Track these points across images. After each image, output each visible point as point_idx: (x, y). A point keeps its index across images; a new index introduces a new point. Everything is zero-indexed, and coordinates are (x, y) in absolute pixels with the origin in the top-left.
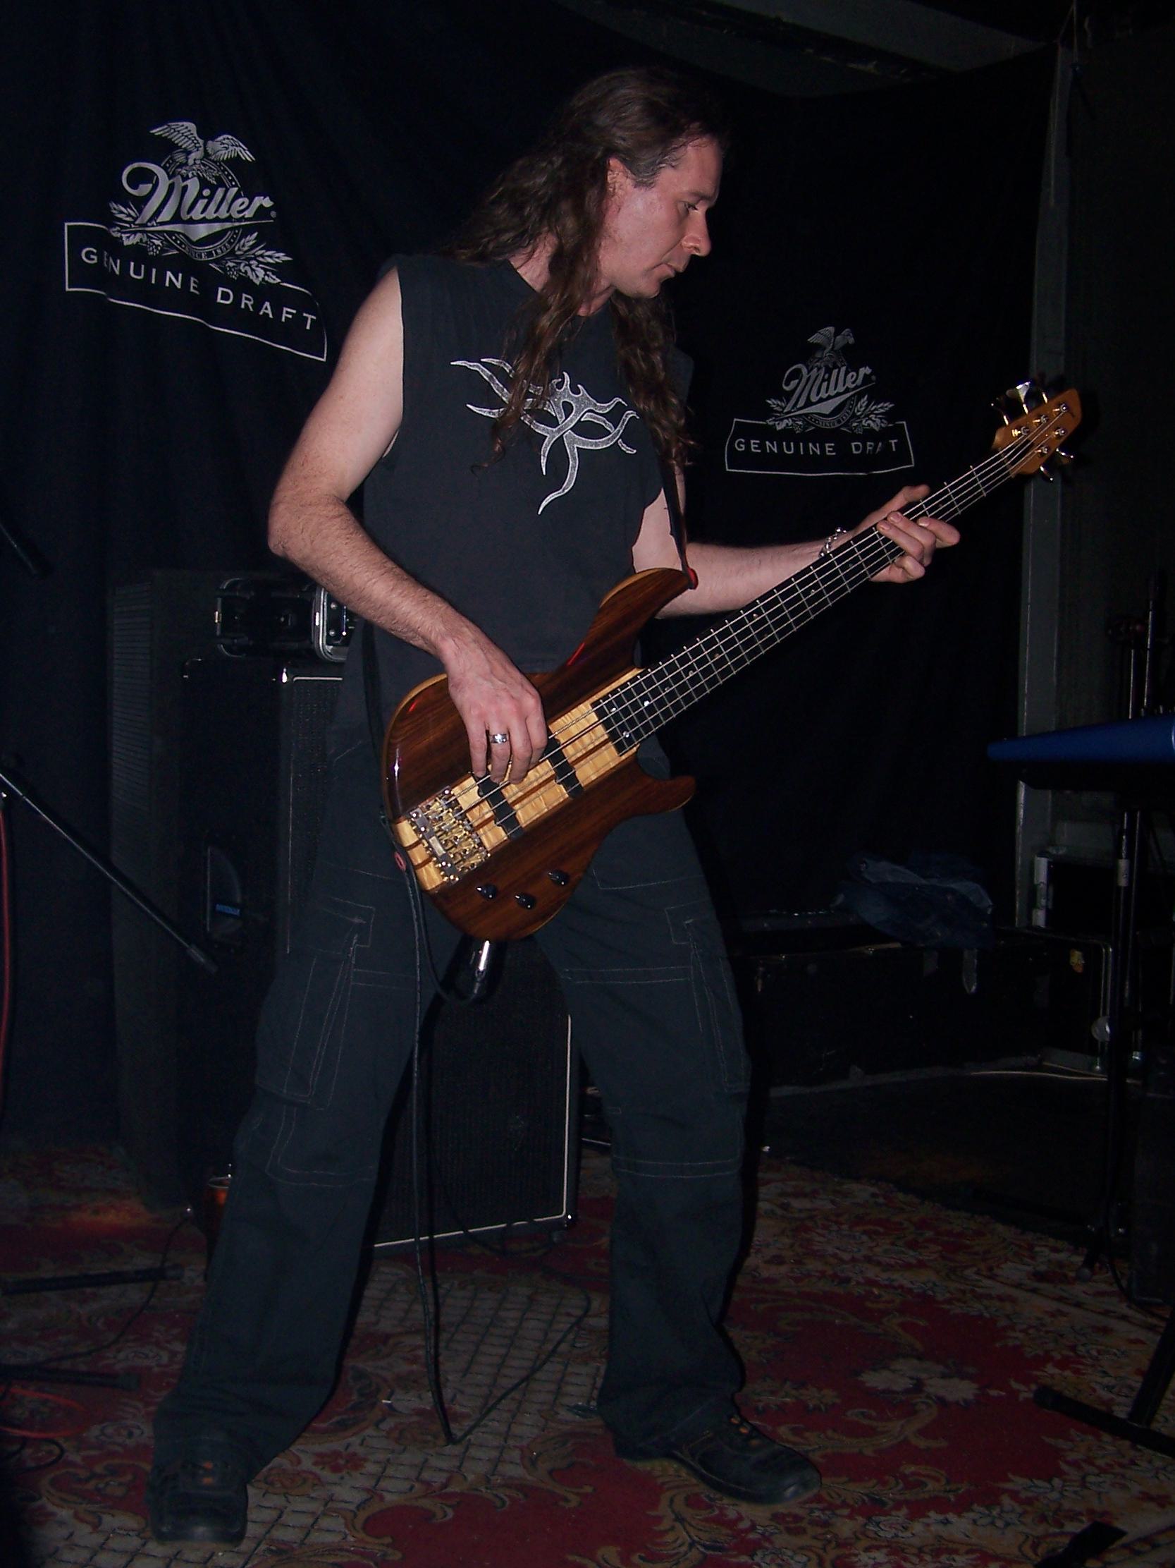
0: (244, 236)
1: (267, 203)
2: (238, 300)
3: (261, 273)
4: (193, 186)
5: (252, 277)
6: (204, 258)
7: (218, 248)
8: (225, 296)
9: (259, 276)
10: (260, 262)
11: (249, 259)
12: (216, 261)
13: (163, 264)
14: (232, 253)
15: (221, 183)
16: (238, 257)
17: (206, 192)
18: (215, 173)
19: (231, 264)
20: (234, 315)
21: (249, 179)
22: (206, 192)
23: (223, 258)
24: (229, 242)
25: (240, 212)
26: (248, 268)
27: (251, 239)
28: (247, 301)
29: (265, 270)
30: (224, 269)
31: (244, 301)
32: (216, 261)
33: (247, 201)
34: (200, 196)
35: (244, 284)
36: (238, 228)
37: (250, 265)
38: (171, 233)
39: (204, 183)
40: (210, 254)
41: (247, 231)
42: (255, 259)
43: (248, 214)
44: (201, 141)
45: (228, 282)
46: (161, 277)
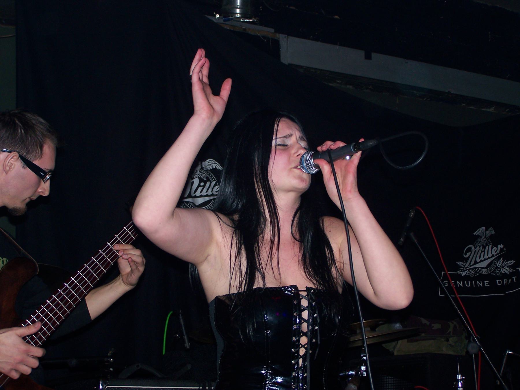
0: (499, 260)
3: (508, 269)
5: (506, 271)
7: (492, 268)
8: (499, 282)
9: (507, 271)
12: (493, 272)
13: (476, 279)
14: (497, 267)
15: (487, 245)
16: (499, 268)
20: (504, 288)
21: (494, 241)
32: (493, 272)
38: (475, 268)
41: (499, 258)
42: (505, 266)
43: (498, 252)
45: (498, 277)
46: (476, 284)
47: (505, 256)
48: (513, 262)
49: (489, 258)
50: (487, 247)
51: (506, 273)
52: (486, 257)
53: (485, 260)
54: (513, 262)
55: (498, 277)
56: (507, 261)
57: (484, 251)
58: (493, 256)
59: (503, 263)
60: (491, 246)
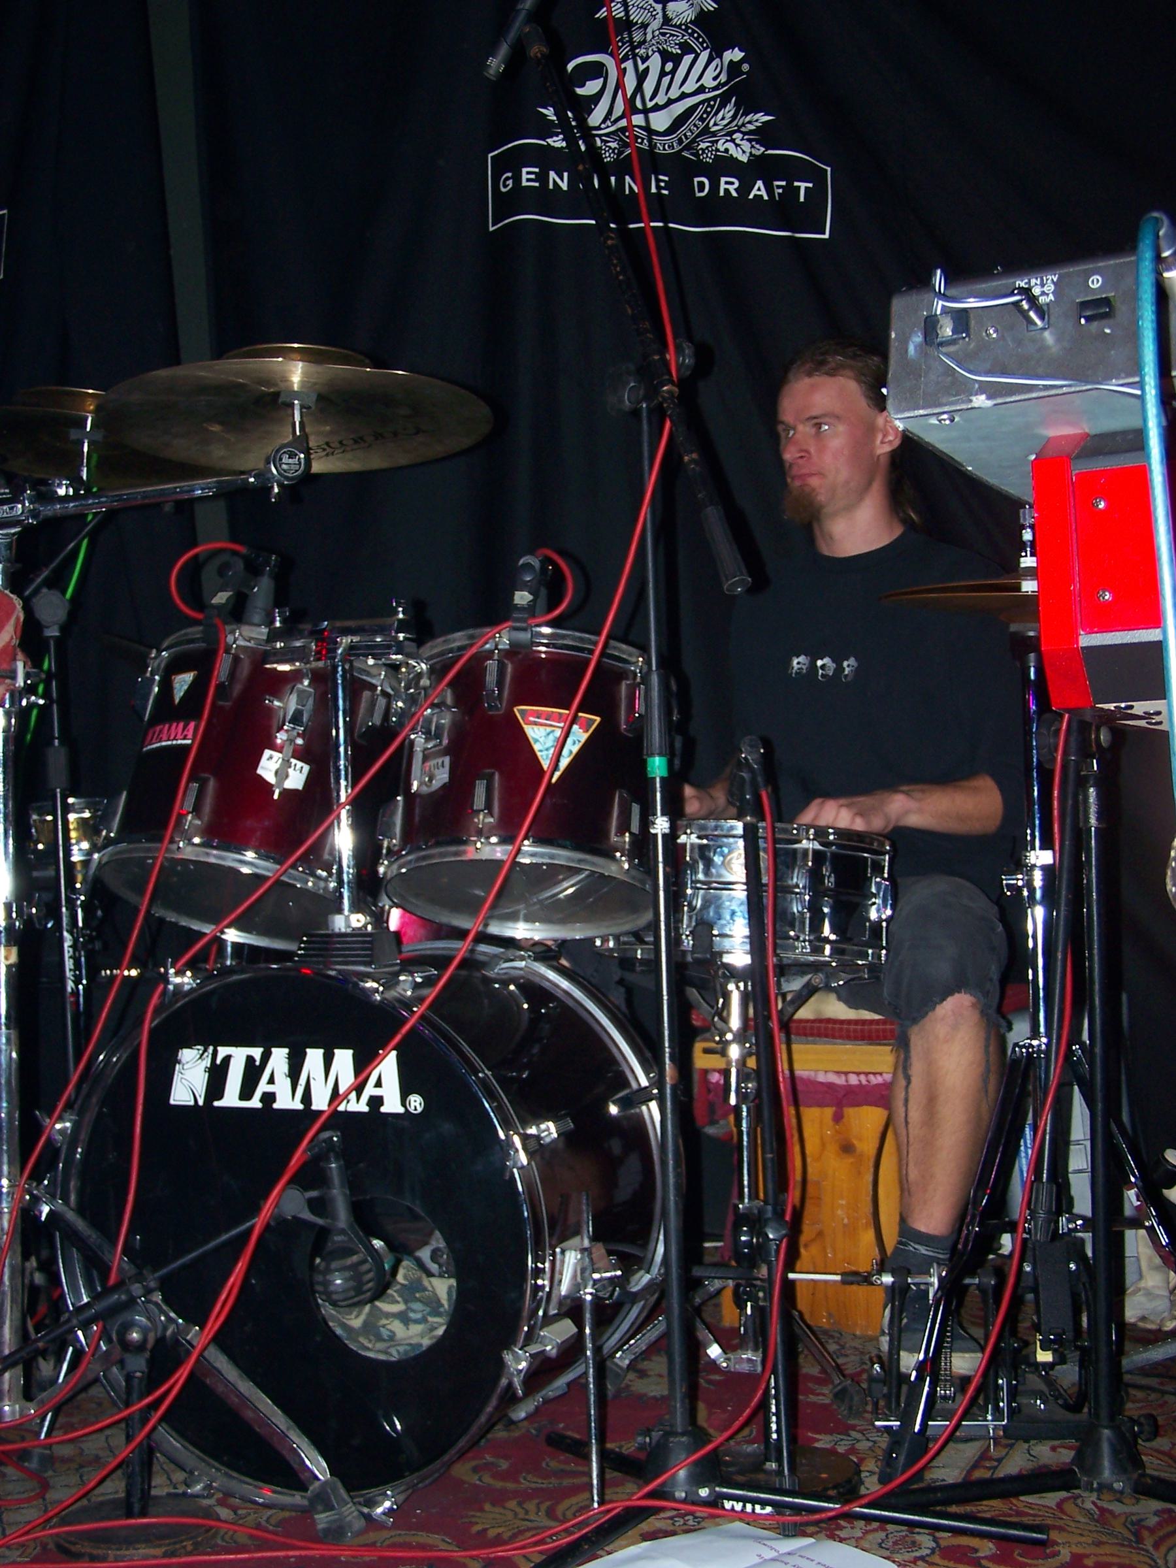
0: (723, 105)
2: (715, 186)
3: (746, 146)
4: (655, 62)
7: (688, 130)
9: (742, 151)
11: (730, 134)
14: (706, 131)
16: (714, 134)
17: (669, 66)
18: (680, 40)
22: (669, 66)
23: (694, 141)
24: (702, 119)
25: (715, 79)
26: (730, 146)
28: (729, 185)
30: (696, 155)
31: (723, 186)
32: (688, 148)
34: (663, 74)
35: (726, 165)
36: (714, 98)
37: (733, 141)
39: (666, 56)
41: (724, 100)
44: (659, 7)
52: (674, 93)
58: (701, 90)
59: (734, 117)
60: (704, 56)
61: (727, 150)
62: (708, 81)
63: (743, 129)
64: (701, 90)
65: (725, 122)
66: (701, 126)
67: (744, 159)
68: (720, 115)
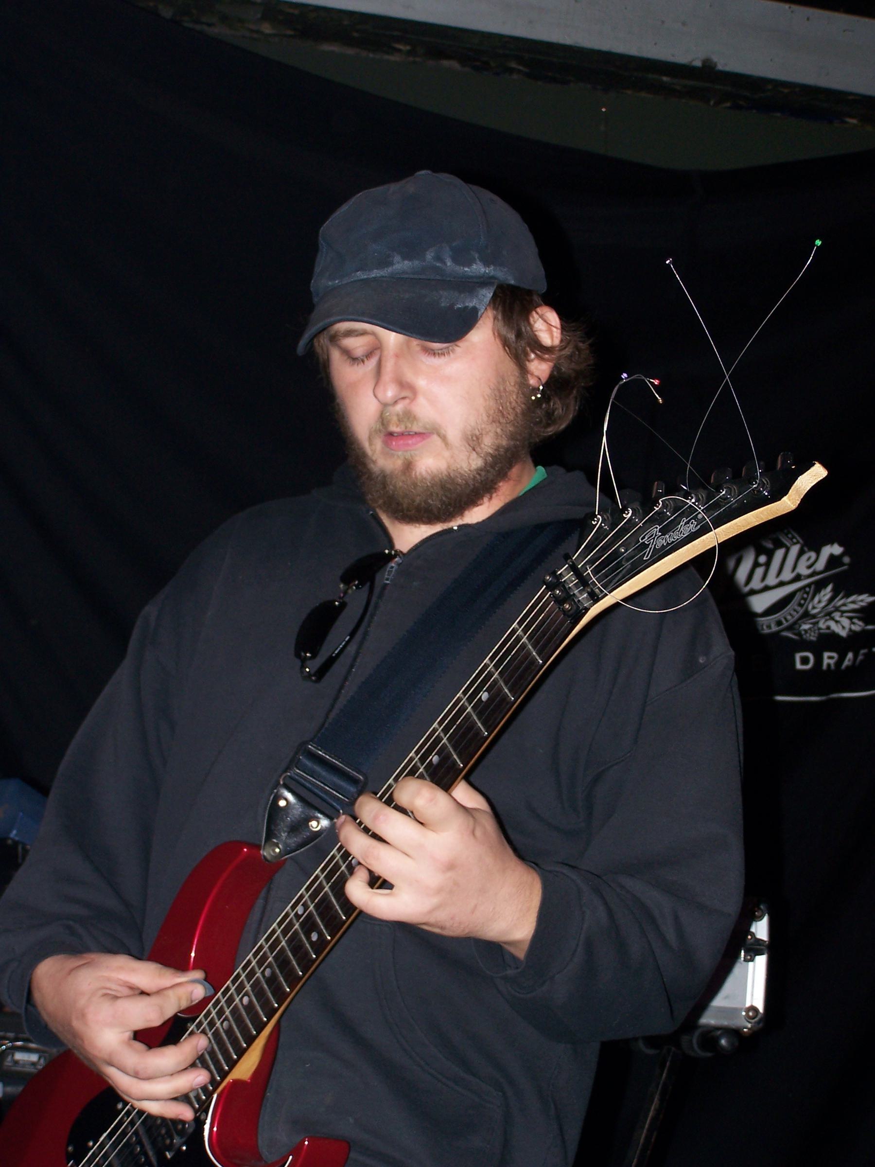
1: (836, 549)
3: (846, 622)
5: (835, 627)
6: (774, 628)
7: (789, 614)
8: (805, 661)
9: (842, 627)
10: (843, 612)
14: (806, 615)
17: (762, 559)
19: (806, 627)
20: (818, 679)
23: (795, 623)
24: (801, 605)
25: (809, 567)
27: (827, 593)
29: (850, 618)
30: (799, 634)
31: (826, 661)
32: (790, 628)
33: (813, 555)
34: (756, 565)
35: (829, 641)
36: (809, 586)
40: (779, 623)
41: (819, 586)
42: (837, 609)
45: (803, 644)
47: (842, 581)
48: (865, 599)
49: (782, 584)
50: (779, 554)
51: (834, 636)
52: (771, 580)
53: (767, 588)
54: (865, 599)
55: (803, 644)
56: (847, 596)
57: (768, 565)
59: (831, 600)
60: (795, 550)
61: (828, 628)
62: (802, 570)
63: (844, 608)
64: (798, 578)
65: (823, 604)
66: (801, 611)
67: (843, 633)
68: (816, 599)
